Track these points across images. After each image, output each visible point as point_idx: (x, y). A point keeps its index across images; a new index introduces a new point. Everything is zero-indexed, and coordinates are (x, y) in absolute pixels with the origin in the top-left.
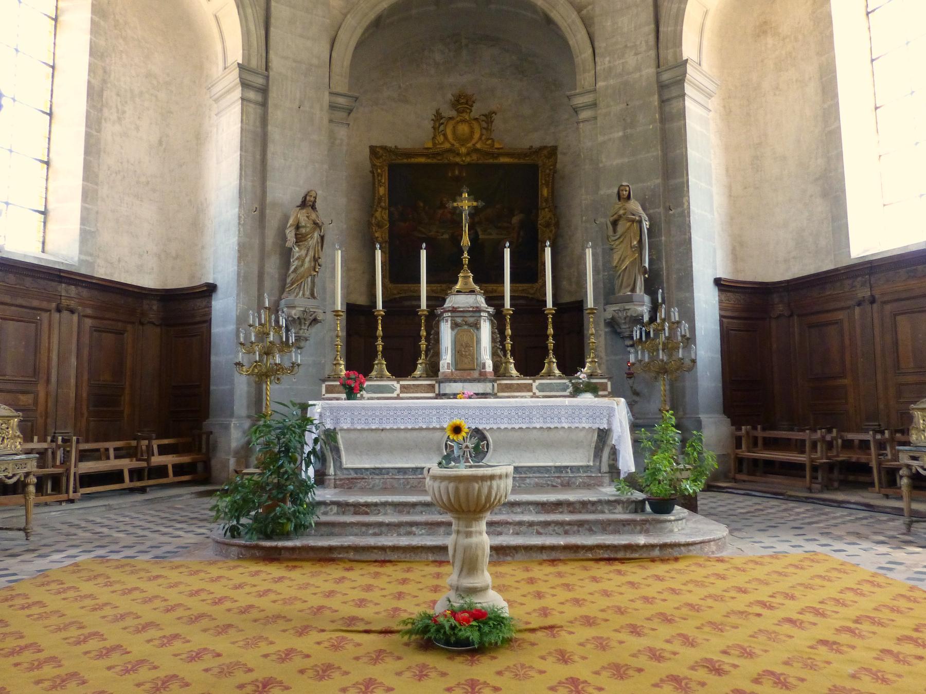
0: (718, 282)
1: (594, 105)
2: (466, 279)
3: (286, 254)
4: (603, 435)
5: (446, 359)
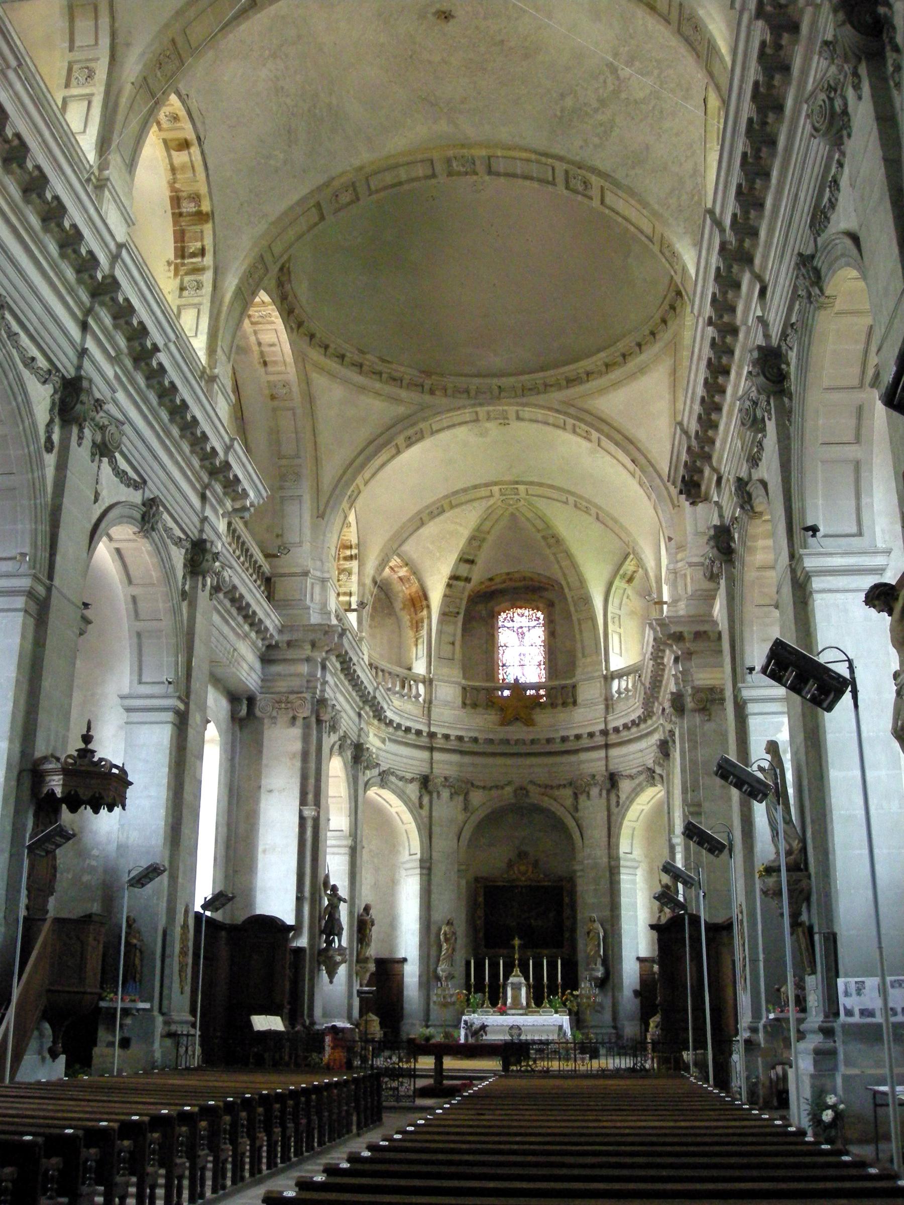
0: (638, 959)
1: (582, 870)
2: (517, 971)
3: (440, 947)
4: (561, 1027)
5: (509, 1000)
